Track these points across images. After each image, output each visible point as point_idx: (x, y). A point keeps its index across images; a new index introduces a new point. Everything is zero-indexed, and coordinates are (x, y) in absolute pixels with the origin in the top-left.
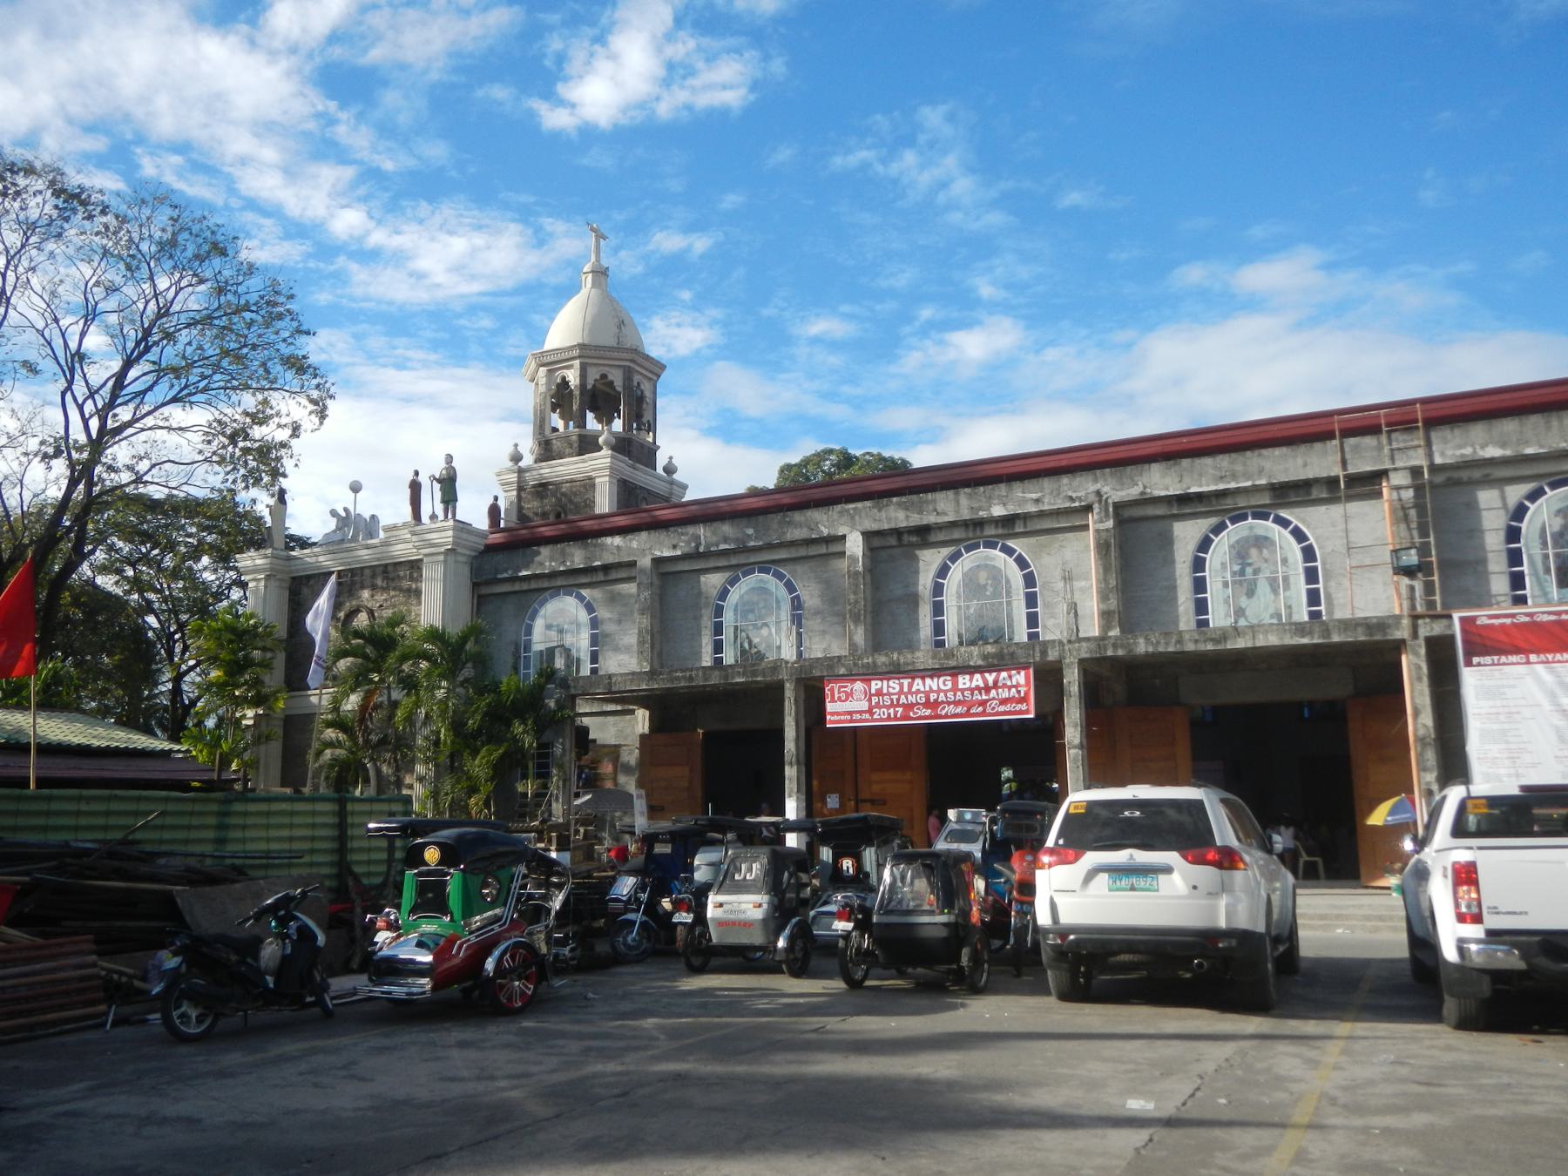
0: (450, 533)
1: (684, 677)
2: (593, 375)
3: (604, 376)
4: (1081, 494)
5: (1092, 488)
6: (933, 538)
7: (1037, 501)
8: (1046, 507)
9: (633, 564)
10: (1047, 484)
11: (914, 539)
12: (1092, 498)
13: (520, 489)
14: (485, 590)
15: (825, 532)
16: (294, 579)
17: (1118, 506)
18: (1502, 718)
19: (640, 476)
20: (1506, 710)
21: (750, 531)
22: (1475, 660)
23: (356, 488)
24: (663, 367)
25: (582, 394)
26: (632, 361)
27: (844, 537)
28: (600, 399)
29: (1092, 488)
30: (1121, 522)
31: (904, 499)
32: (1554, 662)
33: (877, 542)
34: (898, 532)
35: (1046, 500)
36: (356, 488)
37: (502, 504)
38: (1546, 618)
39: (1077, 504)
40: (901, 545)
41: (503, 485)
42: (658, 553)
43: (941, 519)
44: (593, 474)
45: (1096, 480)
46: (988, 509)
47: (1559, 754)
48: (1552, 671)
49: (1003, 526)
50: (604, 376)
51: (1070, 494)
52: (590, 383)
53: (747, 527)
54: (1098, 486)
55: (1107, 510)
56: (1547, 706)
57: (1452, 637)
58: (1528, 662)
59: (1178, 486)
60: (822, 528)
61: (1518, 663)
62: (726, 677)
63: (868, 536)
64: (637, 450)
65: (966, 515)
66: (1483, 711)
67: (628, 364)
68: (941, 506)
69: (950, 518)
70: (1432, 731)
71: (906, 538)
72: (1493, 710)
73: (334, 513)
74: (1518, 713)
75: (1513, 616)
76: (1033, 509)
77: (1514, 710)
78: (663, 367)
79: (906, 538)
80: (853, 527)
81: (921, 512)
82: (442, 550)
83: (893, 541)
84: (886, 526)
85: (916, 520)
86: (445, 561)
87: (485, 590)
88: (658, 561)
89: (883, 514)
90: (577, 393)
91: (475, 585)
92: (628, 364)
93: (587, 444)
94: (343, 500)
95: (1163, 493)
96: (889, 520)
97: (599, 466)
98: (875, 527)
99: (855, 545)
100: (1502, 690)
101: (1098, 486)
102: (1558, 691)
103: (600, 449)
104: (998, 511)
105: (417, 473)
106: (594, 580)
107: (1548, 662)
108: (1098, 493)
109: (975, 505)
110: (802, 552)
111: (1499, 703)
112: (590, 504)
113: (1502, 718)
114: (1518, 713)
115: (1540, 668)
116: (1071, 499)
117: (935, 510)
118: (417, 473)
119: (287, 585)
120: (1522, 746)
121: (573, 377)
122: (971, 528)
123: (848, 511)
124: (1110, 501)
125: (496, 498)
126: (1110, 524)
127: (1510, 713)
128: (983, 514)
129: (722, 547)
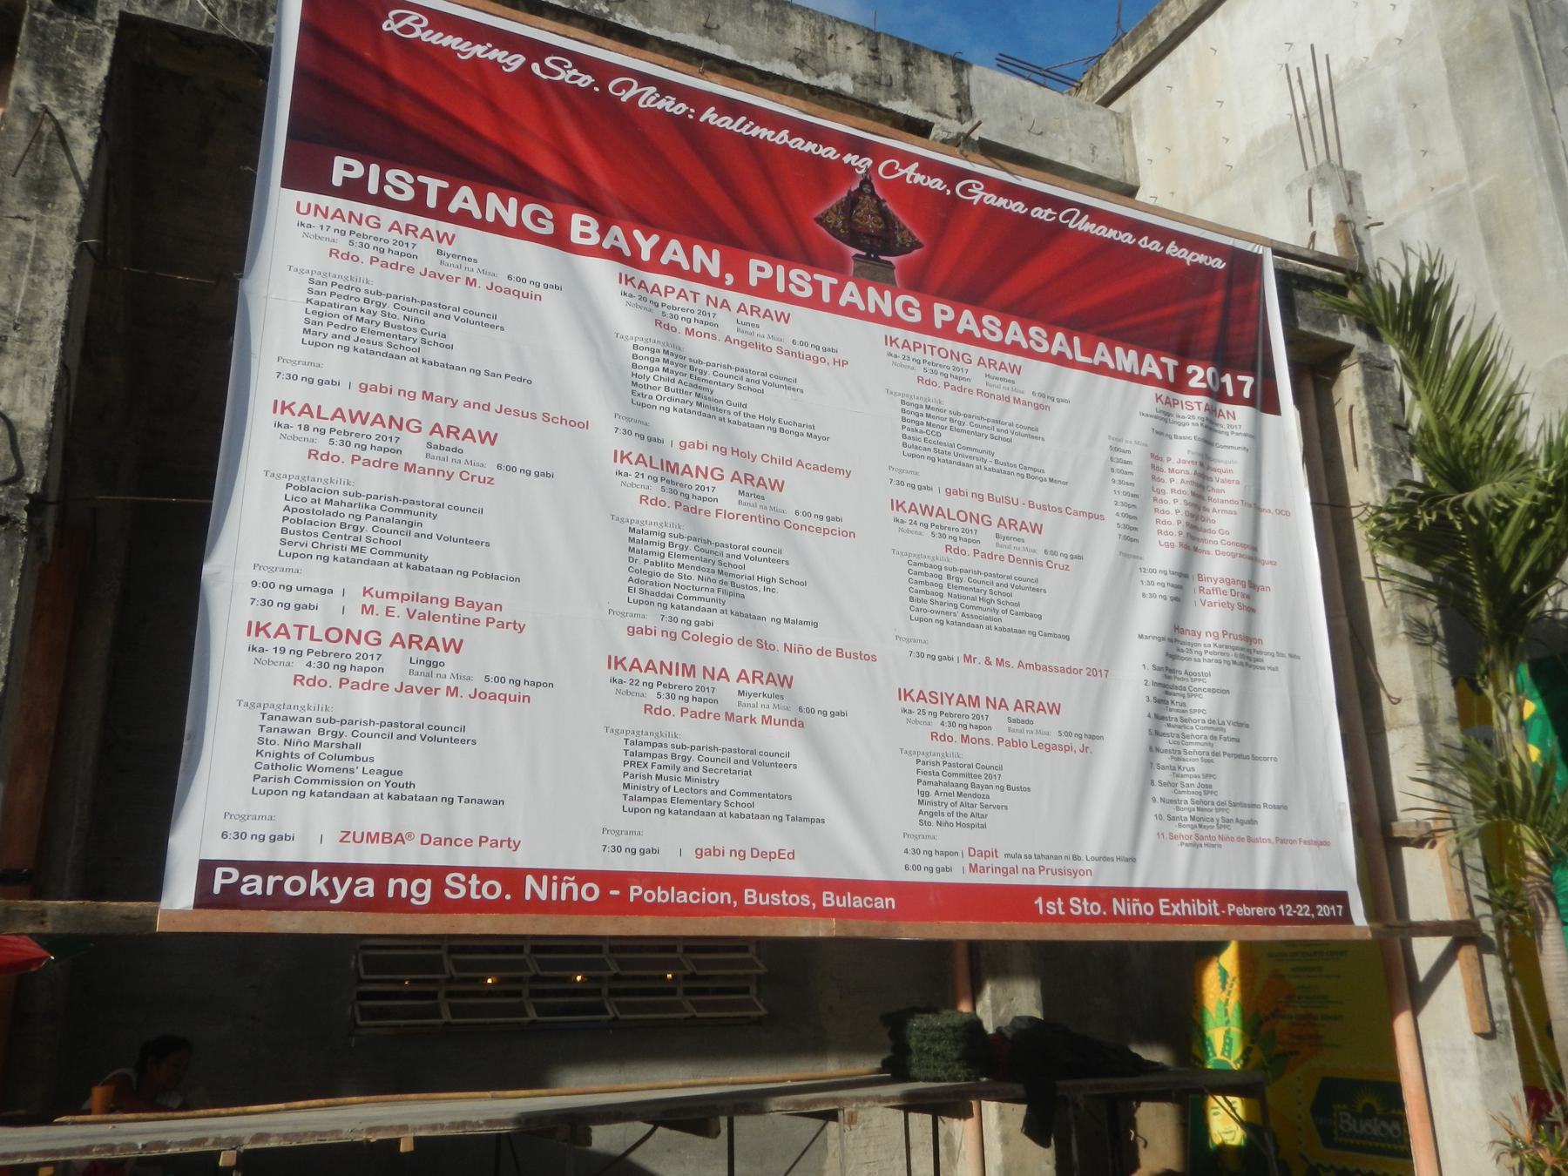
18: (414, 446)
20: (440, 414)
22: (343, 168)
32: (654, 266)
38: (649, 98)
47: (630, 649)
48: (645, 297)
56: (607, 436)
57: (260, 60)
58: (559, 239)
61: (520, 232)
66: (329, 400)
70: (33, 453)
72: (375, 404)
74: (489, 438)
75: (536, 50)
77: (470, 420)
100: (433, 324)
102: (657, 384)
107: (634, 261)
111: (411, 376)
113: (414, 446)
114: (489, 438)
115: (602, 274)
120: (479, 591)
127: (452, 431)
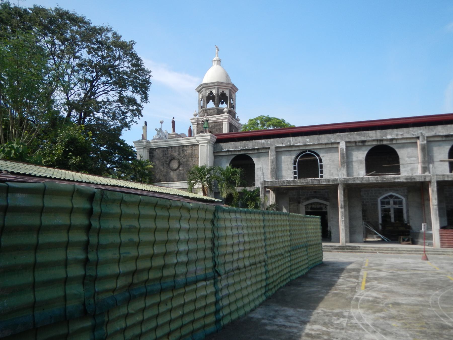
0: (209, 137)
1: (305, 182)
2: (220, 91)
3: (223, 91)
4: (416, 133)
5: (420, 132)
6: (367, 144)
7: (402, 135)
8: (405, 137)
9: (269, 148)
10: (405, 130)
11: (360, 144)
12: (420, 135)
13: (198, 124)
14: (216, 154)
15: (333, 141)
16: (151, 149)
17: (428, 137)
19: (234, 123)
21: (308, 140)
23: (162, 122)
24: (237, 89)
25: (217, 96)
26: (231, 87)
27: (338, 143)
28: (223, 98)
29: (420, 132)
30: (428, 142)
31: (359, 132)
33: (348, 145)
34: (355, 142)
35: (405, 135)
36: (162, 122)
37: (192, 128)
39: (414, 136)
40: (356, 146)
41: (192, 123)
42: (277, 145)
43: (370, 139)
44: (223, 121)
45: (421, 130)
46: (386, 136)
49: (389, 141)
50: (223, 91)
51: (412, 133)
52: (220, 93)
53: (307, 138)
54: (421, 131)
55: (424, 138)
59: (447, 132)
60: (332, 140)
62: (319, 182)
63: (347, 142)
64: (232, 113)
65: (379, 138)
67: (230, 88)
68: (371, 135)
69: (374, 138)
71: (358, 144)
73: (156, 130)
76: (400, 137)
78: (237, 89)
79: (358, 144)
80: (342, 139)
81: (364, 136)
82: (206, 142)
83: (354, 145)
84: (353, 140)
85: (363, 139)
86: (207, 145)
87: (216, 154)
88: (276, 148)
89: (352, 136)
90: (216, 96)
91: (214, 152)
92: (230, 88)
93: (220, 112)
94: (159, 126)
95: (442, 134)
96: (354, 138)
97: (224, 118)
98: (349, 140)
99: (342, 145)
101: (421, 131)
103: (223, 113)
104: (389, 137)
105: (174, 118)
106: (254, 152)
108: (422, 133)
109: (382, 135)
110: (324, 146)
112: (221, 129)
116: (413, 135)
117: (369, 136)
118: (174, 118)
119: (148, 151)
121: (214, 92)
122: (379, 141)
123: (340, 135)
124: (425, 136)
125: (190, 127)
126: (425, 142)
128: (384, 138)
129: (298, 144)
